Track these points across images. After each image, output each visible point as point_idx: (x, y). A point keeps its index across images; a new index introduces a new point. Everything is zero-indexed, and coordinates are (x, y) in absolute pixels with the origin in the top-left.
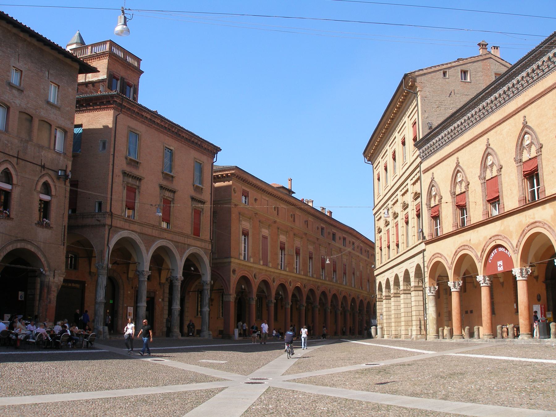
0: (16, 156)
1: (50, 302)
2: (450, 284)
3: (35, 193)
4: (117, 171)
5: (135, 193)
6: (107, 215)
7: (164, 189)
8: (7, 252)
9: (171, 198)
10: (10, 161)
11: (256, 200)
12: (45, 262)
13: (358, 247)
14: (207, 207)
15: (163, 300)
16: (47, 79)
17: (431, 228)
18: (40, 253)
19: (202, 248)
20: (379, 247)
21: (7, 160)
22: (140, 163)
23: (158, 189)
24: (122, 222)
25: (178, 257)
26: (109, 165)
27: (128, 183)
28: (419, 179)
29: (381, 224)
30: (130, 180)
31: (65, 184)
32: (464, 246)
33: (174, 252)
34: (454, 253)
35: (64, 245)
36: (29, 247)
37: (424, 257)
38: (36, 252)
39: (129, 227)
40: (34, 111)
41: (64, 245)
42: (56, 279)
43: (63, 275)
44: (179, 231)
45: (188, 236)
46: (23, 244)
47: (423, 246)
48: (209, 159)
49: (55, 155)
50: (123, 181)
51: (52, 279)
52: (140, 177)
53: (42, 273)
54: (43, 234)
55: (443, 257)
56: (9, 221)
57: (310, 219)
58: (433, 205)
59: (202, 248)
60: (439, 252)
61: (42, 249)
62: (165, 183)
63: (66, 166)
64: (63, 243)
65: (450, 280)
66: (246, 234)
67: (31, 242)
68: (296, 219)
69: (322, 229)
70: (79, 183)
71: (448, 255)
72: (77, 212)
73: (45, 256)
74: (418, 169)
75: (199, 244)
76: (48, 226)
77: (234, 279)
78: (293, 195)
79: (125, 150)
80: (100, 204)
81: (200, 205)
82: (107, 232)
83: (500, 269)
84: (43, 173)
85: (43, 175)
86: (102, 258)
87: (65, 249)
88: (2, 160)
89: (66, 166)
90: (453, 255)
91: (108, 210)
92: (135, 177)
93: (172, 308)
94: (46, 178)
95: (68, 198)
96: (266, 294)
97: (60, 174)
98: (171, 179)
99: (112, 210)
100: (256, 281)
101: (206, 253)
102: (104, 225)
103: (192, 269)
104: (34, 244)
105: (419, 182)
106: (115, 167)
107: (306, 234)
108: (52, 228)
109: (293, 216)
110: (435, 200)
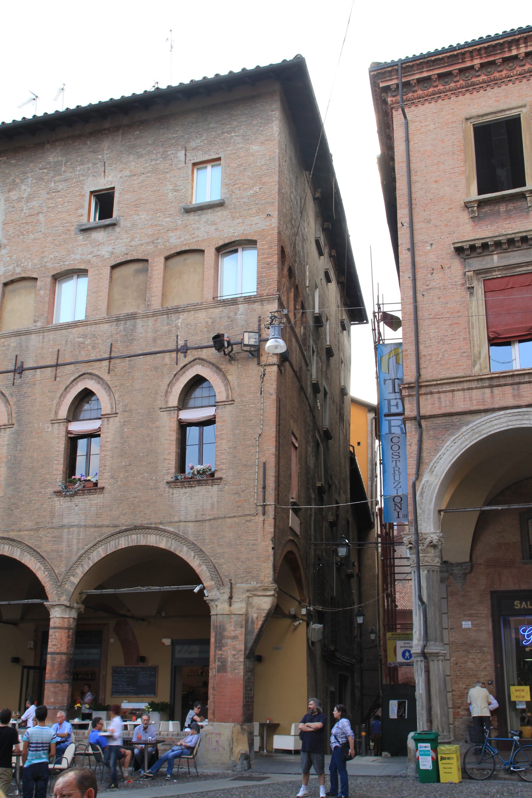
3: (164, 415)
8: (91, 564)
10: (88, 373)
12: (204, 567)
16: (183, 165)
18: (185, 549)
31: (259, 364)
38: (172, 550)
40: (151, 247)
42: (239, 607)
43: (266, 590)
46: (134, 536)
49: (217, 312)
51: (226, 605)
64: (260, 508)
67: (156, 529)
73: (200, 552)
84: (181, 365)
92: (473, 248)
104: (165, 531)
108: (221, 479)
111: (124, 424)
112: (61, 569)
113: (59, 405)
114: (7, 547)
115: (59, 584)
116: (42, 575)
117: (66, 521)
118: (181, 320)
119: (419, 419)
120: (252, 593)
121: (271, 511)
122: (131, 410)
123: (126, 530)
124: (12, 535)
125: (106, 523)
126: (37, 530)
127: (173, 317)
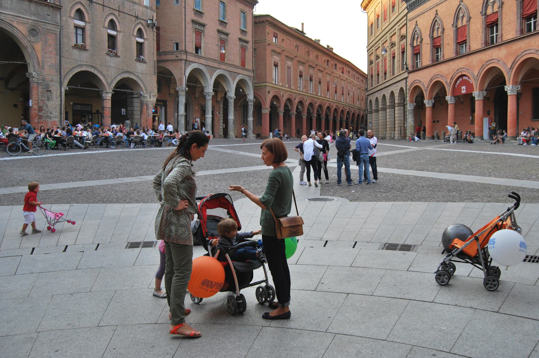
0: (118, 9)
1: (148, 115)
2: (426, 101)
4: (188, 19)
5: (201, 35)
6: (183, 53)
7: (220, 32)
9: (225, 39)
11: (283, 40)
13: (352, 75)
14: (250, 46)
15: (219, 113)
17: (413, 62)
19: (247, 75)
20: (371, 74)
21: (112, 13)
22: (204, 13)
23: (216, 32)
24: (193, 57)
25: (231, 82)
26: (182, 15)
27: (196, 28)
28: (406, 24)
29: (373, 58)
30: (197, 26)
32: (437, 75)
33: (229, 78)
34: (429, 80)
35: (155, 75)
36: (132, 76)
37: (406, 82)
38: (137, 80)
39: (198, 60)
41: (155, 75)
42: (152, 100)
44: (231, 63)
45: (237, 67)
46: (128, 74)
47: (406, 75)
48: (250, 9)
49: (144, 8)
50: (193, 27)
52: (204, 24)
53: (141, 95)
54: (140, 67)
55: (421, 83)
56: (117, 58)
57: (319, 54)
58: (415, 44)
59: (247, 75)
60: (417, 79)
61: (141, 78)
62: (220, 28)
63: (153, 16)
65: (425, 99)
66: (276, 65)
68: (310, 54)
69: (328, 61)
70: (160, 29)
71: (425, 81)
72: (160, 51)
73: (143, 83)
74: (405, 18)
75: (245, 72)
76: (143, 61)
77: (269, 97)
78: (305, 35)
79: (193, 3)
80: (177, 44)
81: (245, 44)
82: (184, 65)
83: (464, 92)
84: (137, 22)
85: (138, 23)
86: (181, 84)
87: (156, 78)
88: (108, 13)
89: (153, 16)
90: (428, 81)
91: (184, 49)
93: (228, 118)
94: (140, 26)
95: (156, 40)
96: (290, 108)
97: (149, 23)
98: (225, 25)
99: (186, 49)
100: (283, 98)
101: (250, 79)
102: (181, 60)
103: (241, 90)
104: (135, 75)
105: (405, 26)
106: (187, 16)
107: (316, 65)
109: (308, 53)
110: (417, 41)
111: (124, 36)
112: (109, 81)
113: (105, 21)
114: (92, 69)
115: (109, 85)
116: (104, 81)
117: (110, 65)
118: (136, 7)
119: (186, 60)
120: (153, 96)
121: (156, 74)
122: (125, 32)
123: (126, 72)
124: (94, 65)
125: (120, 68)
126: (102, 66)
127: (134, 5)
